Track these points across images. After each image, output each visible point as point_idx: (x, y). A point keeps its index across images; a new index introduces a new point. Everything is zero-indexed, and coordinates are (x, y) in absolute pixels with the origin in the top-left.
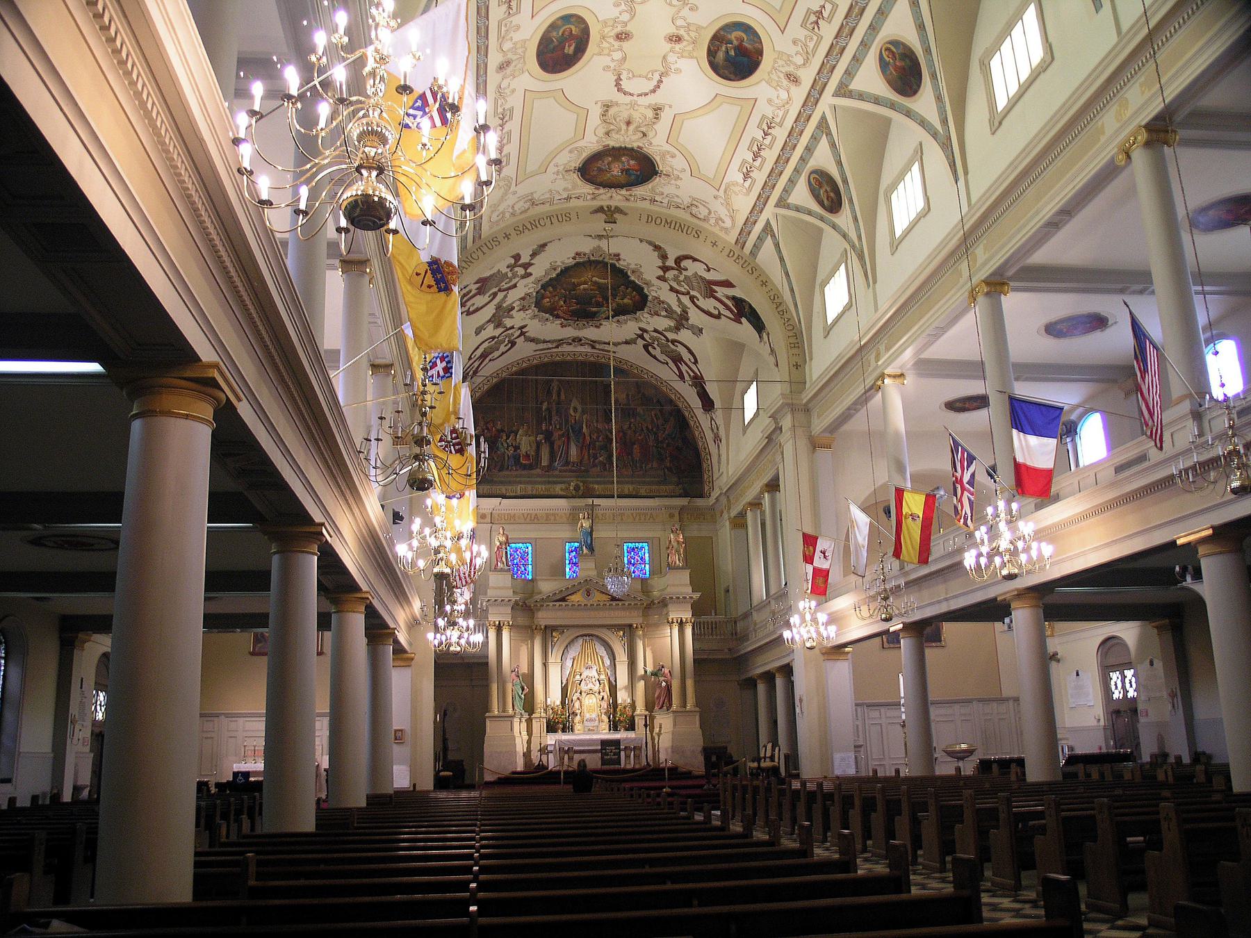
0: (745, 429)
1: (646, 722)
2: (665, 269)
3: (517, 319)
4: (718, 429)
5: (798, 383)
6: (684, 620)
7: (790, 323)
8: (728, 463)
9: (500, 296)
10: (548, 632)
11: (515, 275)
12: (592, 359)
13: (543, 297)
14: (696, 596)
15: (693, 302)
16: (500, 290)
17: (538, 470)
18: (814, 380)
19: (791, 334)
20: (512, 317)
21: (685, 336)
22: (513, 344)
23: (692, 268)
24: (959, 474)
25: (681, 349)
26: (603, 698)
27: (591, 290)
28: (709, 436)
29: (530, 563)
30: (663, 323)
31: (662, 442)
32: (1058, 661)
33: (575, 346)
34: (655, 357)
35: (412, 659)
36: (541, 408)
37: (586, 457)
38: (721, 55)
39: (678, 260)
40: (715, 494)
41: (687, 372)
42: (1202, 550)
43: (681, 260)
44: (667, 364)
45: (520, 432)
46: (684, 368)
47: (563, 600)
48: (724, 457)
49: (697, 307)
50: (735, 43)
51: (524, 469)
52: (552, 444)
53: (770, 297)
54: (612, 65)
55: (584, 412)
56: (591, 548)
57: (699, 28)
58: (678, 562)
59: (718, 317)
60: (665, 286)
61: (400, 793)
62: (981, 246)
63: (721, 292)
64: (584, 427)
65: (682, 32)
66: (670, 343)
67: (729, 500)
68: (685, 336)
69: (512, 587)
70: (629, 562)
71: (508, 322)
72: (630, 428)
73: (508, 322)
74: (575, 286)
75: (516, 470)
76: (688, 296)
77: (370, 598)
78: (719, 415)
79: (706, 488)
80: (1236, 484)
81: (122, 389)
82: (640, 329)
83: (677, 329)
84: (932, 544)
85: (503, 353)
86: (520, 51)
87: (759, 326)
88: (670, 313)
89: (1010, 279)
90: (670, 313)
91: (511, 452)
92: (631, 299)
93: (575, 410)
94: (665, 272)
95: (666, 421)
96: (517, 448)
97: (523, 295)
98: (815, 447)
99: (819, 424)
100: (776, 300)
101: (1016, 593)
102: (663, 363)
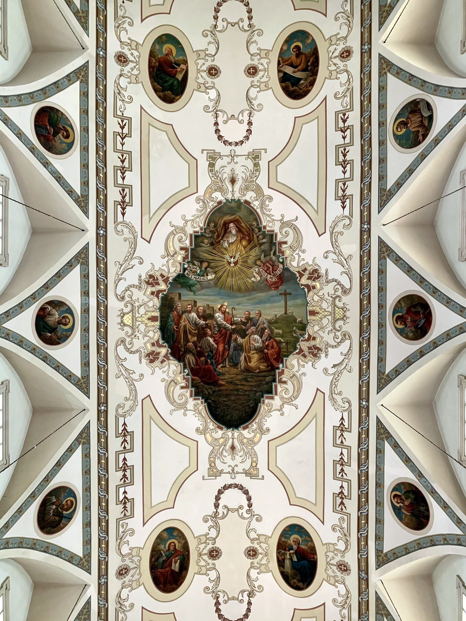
38: (287, 563)
50: (295, 547)
54: (211, 585)
57: (267, 537)
65: (256, 545)
86: (136, 559)
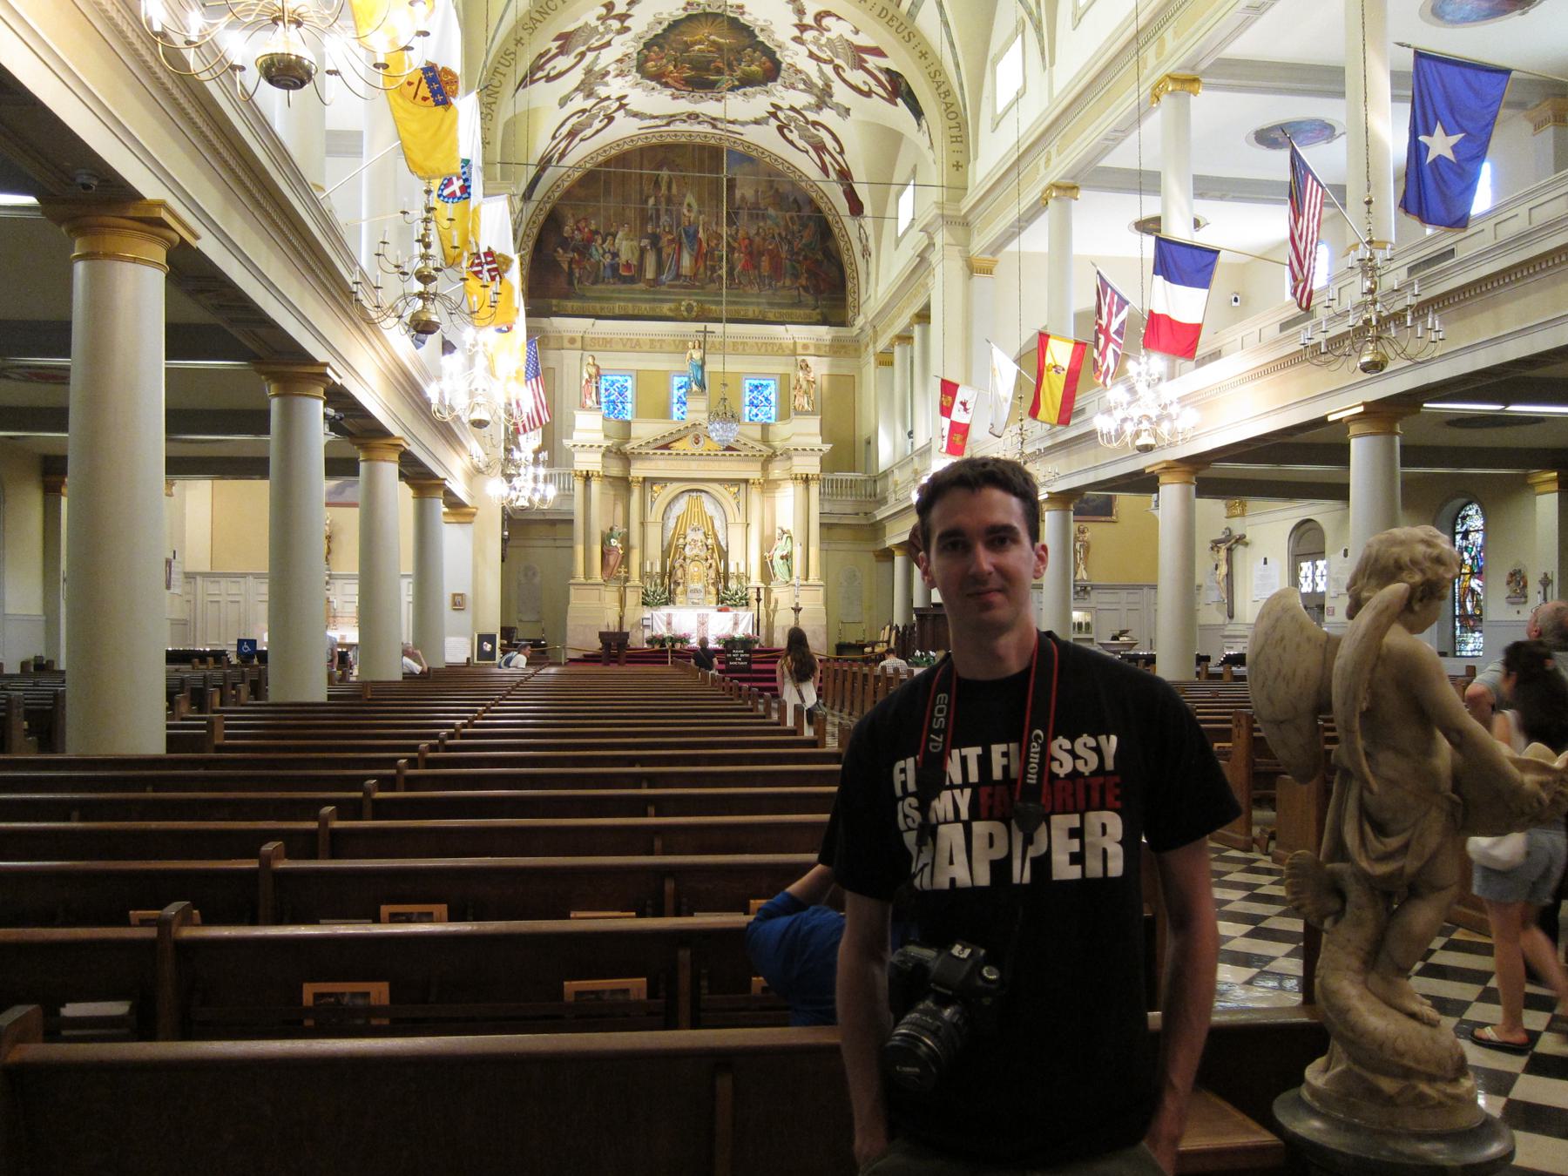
0: (898, 241)
1: (758, 595)
2: (803, 28)
3: (614, 87)
4: (867, 240)
5: (957, 189)
6: (810, 476)
7: (951, 109)
8: (877, 284)
9: (590, 56)
10: (648, 485)
11: (608, 30)
12: (713, 142)
13: (647, 59)
14: (827, 447)
15: (839, 74)
16: (589, 49)
17: (641, 286)
18: (978, 182)
19: (953, 123)
20: (606, 84)
21: (827, 116)
22: (610, 119)
23: (836, 29)
24: (1104, 322)
25: (823, 134)
26: (711, 566)
27: (709, 52)
28: (857, 248)
29: (629, 400)
30: (801, 99)
31: (798, 254)
32: (1246, 544)
33: (691, 124)
34: (791, 143)
35: (473, 515)
36: (646, 201)
37: (702, 270)
39: (819, 17)
40: (860, 321)
41: (832, 164)
42: (1353, 429)
43: (823, 17)
46: (827, 159)
47: (666, 447)
48: (873, 277)
49: (844, 81)
52: (659, 252)
53: (929, 73)
55: (700, 212)
56: (702, 385)
58: (806, 406)
59: (868, 94)
60: (803, 51)
61: (453, 668)
62: (1171, 30)
63: (872, 62)
64: (701, 231)
66: (810, 127)
67: (875, 332)
68: (827, 116)
69: (604, 429)
70: (752, 404)
71: (602, 91)
72: (758, 234)
73: (602, 91)
74: (688, 46)
75: (614, 284)
76: (831, 66)
77: (404, 444)
78: (868, 224)
79: (850, 314)
80: (1366, 359)
81: (60, 226)
82: (773, 105)
83: (819, 107)
84: (1077, 398)
85: (597, 132)
87: (917, 112)
88: (809, 86)
89: (1204, 73)
90: (809, 86)
91: (608, 259)
92: (760, 66)
94: (802, 32)
95: (805, 226)
96: (615, 255)
97: (620, 56)
98: (972, 272)
99: (980, 243)
100: (935, 74)
101: (1164, 465)
102: (802, 151)
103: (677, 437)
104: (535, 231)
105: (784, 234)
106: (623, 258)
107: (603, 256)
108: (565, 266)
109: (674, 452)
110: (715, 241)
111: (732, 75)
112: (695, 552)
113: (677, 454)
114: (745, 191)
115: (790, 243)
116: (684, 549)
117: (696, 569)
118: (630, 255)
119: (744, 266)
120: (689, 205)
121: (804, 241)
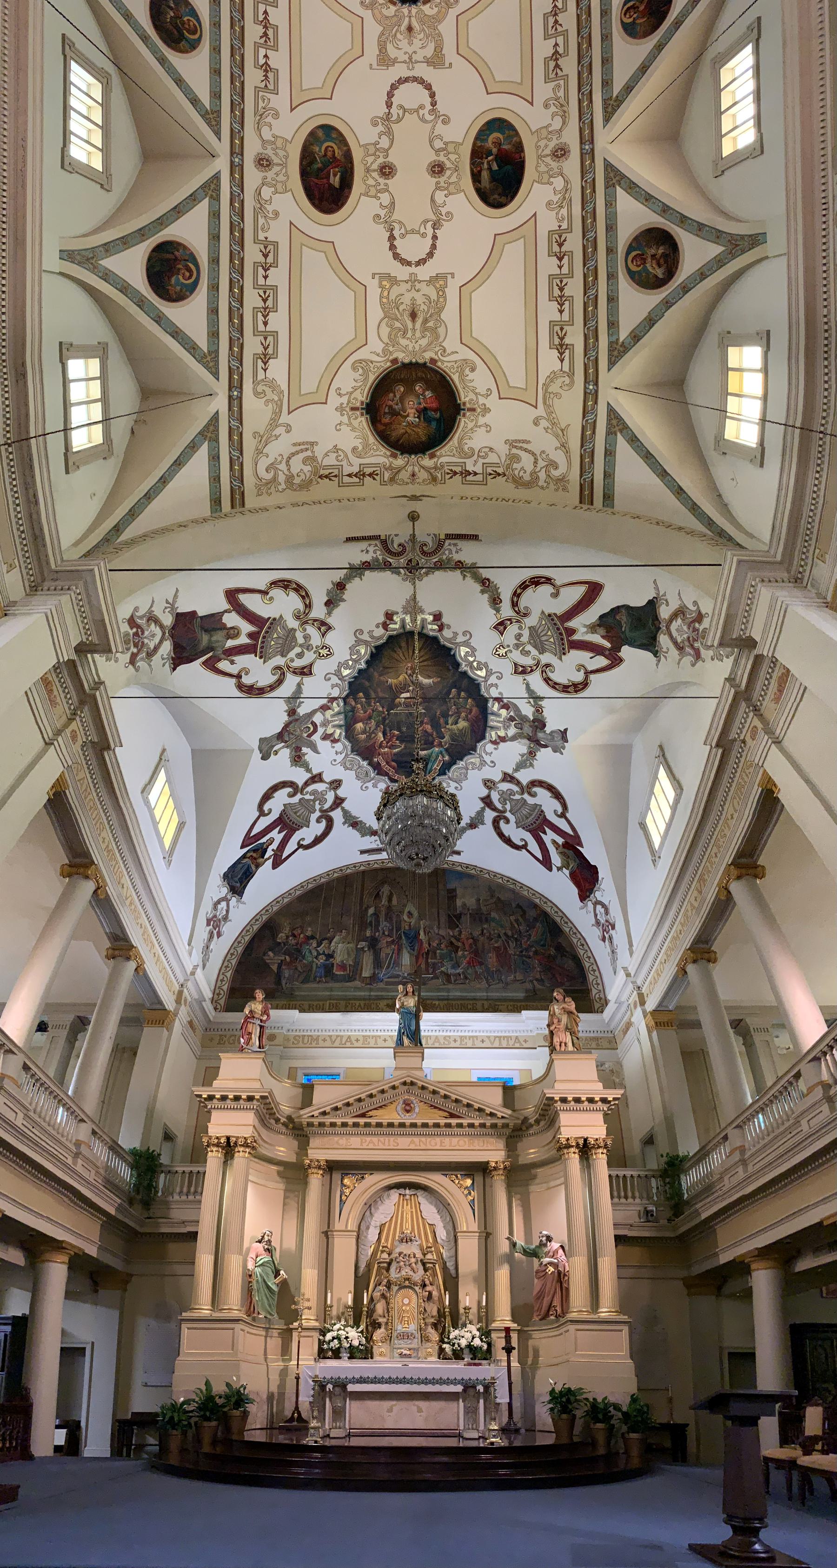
10: (337, 1176)
17: (357, 983)
28: (591, 935)
31: (527, 950)
37: (423, 966)
44: (525, 847)
45: (335, 940)
47: (363, 1115)
51: (337, 981)
55: (421, 917)
64: (422, 933)
72: (482, 934)
91: (322, 959)
93: (410, 914)
95: (531, 926)
96: (330, 956)
103: (378, 1100)
104: (247, 938)
105: (510, 933)
106: (338, 959)
107: (316, 958)
108: (275, 968)
109: (373, 1121)
110: (437, 942)
111: (440, 745)
112: (406, 1272)
113: (379, 1125)
114: (466, 900)
115: (516, 940)
116: (388, 1269)
117: (406, 1301)
118: (346, 957)
119: (469, 963)
120: (409, 912)
121: (532, 939)
